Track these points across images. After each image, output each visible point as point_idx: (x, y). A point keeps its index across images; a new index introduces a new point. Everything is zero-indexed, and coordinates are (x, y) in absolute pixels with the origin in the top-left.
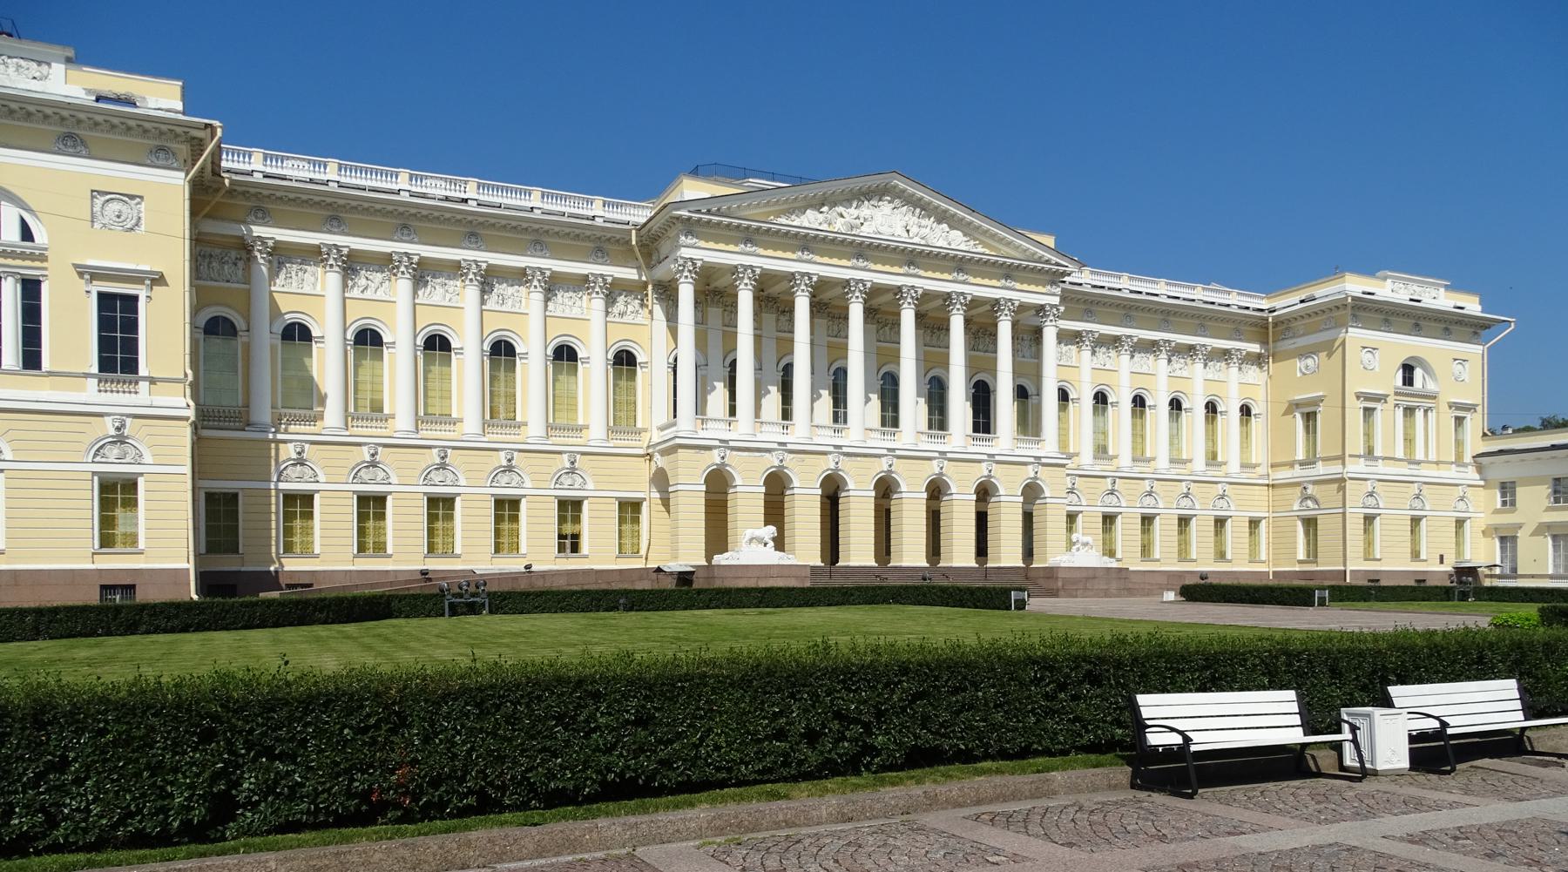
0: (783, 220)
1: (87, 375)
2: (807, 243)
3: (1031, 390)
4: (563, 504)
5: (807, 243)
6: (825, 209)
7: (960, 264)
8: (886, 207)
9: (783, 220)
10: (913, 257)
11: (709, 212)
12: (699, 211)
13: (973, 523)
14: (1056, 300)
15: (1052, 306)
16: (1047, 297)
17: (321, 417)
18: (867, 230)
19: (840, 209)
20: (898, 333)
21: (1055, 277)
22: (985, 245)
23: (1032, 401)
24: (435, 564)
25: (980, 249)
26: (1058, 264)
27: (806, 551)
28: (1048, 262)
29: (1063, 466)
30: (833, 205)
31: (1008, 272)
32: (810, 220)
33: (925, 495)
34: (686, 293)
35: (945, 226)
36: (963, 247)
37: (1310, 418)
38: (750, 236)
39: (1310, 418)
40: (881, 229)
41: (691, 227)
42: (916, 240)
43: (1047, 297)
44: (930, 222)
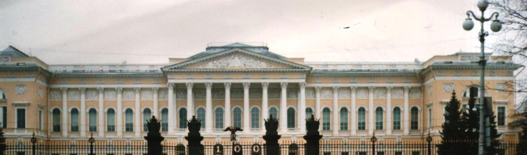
0: (201, 67)
8: (237, 59)
14: (304, 81)
15: (302, 83)
19: (220, 61)
25: (273, 67)
26: (302, 68)
28: (298, 68)
32: (210, 66)
35: (259, 62)
36: (265, 67)
37: (430, 110)
39: (430, 110)
40: (235, 65)
42: (248, 67)
44: (252, 60)
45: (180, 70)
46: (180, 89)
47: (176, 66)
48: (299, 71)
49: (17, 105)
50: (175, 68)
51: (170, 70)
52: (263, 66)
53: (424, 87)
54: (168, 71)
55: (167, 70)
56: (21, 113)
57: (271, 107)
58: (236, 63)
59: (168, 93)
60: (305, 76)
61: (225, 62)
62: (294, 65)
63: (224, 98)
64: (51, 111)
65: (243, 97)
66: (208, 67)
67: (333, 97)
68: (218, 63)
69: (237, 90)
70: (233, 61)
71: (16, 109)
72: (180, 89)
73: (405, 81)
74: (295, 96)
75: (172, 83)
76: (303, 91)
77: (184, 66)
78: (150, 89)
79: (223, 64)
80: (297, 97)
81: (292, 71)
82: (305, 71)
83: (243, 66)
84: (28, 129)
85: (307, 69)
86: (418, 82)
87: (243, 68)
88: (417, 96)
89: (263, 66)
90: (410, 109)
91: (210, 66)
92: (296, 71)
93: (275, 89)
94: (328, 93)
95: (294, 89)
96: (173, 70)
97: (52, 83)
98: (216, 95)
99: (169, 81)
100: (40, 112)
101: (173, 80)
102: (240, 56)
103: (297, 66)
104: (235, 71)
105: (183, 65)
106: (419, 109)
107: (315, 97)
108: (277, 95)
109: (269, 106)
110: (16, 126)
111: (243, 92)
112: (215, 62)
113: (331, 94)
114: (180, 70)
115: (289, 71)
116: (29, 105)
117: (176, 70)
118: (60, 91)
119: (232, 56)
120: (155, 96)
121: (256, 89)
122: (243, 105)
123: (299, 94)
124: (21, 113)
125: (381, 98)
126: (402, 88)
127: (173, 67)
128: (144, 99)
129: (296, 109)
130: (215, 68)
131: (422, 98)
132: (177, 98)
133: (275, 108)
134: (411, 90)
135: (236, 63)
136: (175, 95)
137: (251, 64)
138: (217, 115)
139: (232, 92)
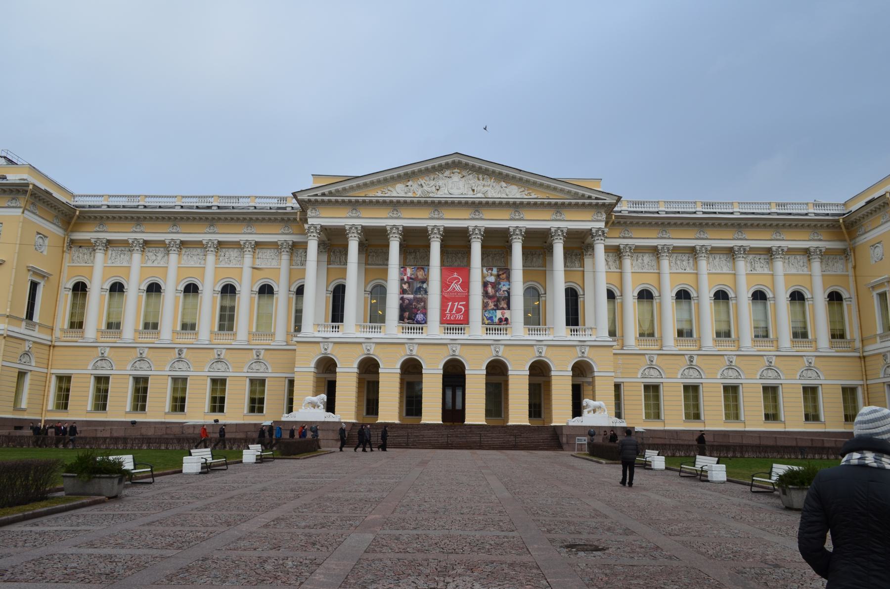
0: (379, 194)
1: (22, 320)
2: (396, 205)
3: (617, 293)
4: (214, 381)
5: (396, 205)
7: (516, 206)
8: (456, 178)
10: (477, 206)
12: (316, 195)
13: (570, 393)
14: (602, 225)
17: (273, 335)
18: (440, 194)
19: (422, 181)
20: (387, 260)
23: (618, 300)
24: (139, 418)
25: (533, 196)
26: (597, 198)
27: (347, 411)
28: (590, 198)
29: (612, 346)
31: (558, 207)
32: (399, 191)
33: (485, 372)
34: (313, 246)
35: (504, 184)
37: (883, 296)
44: (491, 182)
45: (333, 198)
46: (333, 243)
47: (326, 191)
48: (590, 205)
50: (323, 195)
51: (313, 198)
52: (514, 193)
53: (854, 250)
54: (309, 201)
55: (305, 197)
58: (455, 186)
60: (604, 216)
61: (432, 183)
62: (581, 192)
64: (70, 285)
66: (395, 194)
67: (659, 268)
69: (456, 244)
70: (450, 181)
73: (812, 237)
77: (344, 189)
78: (274, 245)
81: (577, 205)
82: (604, 204)
83: (471, 192)
85: (609, 201)
86: (845, 240)
88: (838, 268)
89: (514, 193)
91: (399, 191)
92: (583, 204)
94: (647, 258)
95: (579, 246)
96: (319, 198)
97: (72, 231)
99: (310, 221)
101: (319, 219)
102: (464, 173)
104: (453, 203)
105: (340, 187)
106: (845, 295)
107: (621, 266)
109: (524, 283)
112: (409, 183)
113: (654, 263)
114: (333, 198)
115: (570, 204)
117: (326, 198)
118: (91, 246)
119: (447, 173)
120: (285, 257)
123: (587, 261)
125: (759, 270)
126: (806, 252)
127: (319, 192)
128: (259, 263)
129: (580, 292)
130: (410, 194)
131: (851, 272)
133: (535, 289)
134: (826, 255)
135: (455, 186)
136: (325, 257)
137: (486, 188)
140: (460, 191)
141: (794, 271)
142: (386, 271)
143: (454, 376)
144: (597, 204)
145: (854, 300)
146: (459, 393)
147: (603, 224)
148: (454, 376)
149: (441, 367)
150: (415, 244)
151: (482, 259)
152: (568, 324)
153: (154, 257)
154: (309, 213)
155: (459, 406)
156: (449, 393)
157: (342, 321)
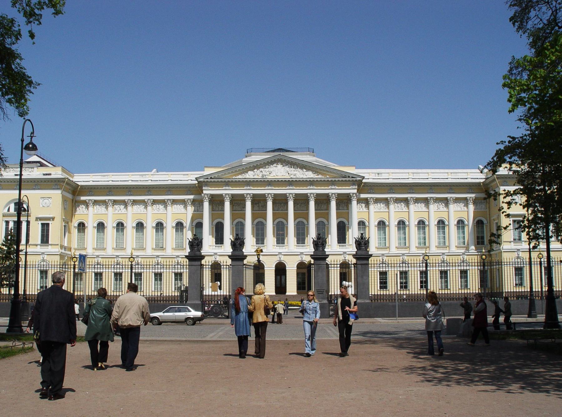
6: (255, 170)
8: (280, 166)
9: (240, 177)
11: (211, 178)
14: (355, 191)
16: (352, 190)
19: (261, 169)
21: (353, 183)
22: (322, 174)
26: (352, 177)
30: (258, 169)
31: (333, 183)
32: (250, 175)
33: (296, 268)
34: (206, 205)
35: (305, 170)
38: (228, 184)
40: (277, 174)
41: (207, 184)
42: (292, 176)
43: (352, 190)
46: (217, 202)
48: (349, 180)
49: (41, 219)
50: (211, 178)
52: (310, 175)
55: (202, 180)
56: (45, 228)
57: (319, 220)
59: (203, 205)
60: (356, 187)
61: (267, 170)
63: (266, 210)
65: (287, 210)
68: (259, 171)
69: (280, 202)
71: (40, 222)
72: (217, 202)
74: (345, 208)
75: (207, 194)
76: (354, 203)
79: (264, 173)
80: (348, 209)
82: (356, 180)
84: (51, 245)
87: (287, 177)
89: (310, 175)
90: (475, 222)
91: (250, 175)
93: (323, 202)
95: (344, 202)
98: (256, 208)
99: (204, 192)
100: (65, 226)
102: (284, 164)
103: (347, 175)
106: (485, 222)
108: (325, 207)
109: (316, 219)
110: (39, 242)
111: (287, 203)
116: (53, 219)
119: (275, 165)
121: (302, 202)
122: (286, 219)
124: (45, 228)
125: (442, 209)
130: (256, 177)
132: (213, 210)
137: (295, 172)
138: (257, 230)
139: (274, 203)
140: (282, 174)
141: (459, 209)
142: (244, 215)
143: (281, 270)
144: (353, 180)
145: (488, 224)
146: (283, 277)
147: (356, 190)
148: (281, 270)
149: (274, 266)
150: (259, 202)
151: (294, 207)
152: (338, 243)
153: (119, 209)
154: (204, 188)
155: (283, 285)
156: (279, 277)
157: (223, 244)
